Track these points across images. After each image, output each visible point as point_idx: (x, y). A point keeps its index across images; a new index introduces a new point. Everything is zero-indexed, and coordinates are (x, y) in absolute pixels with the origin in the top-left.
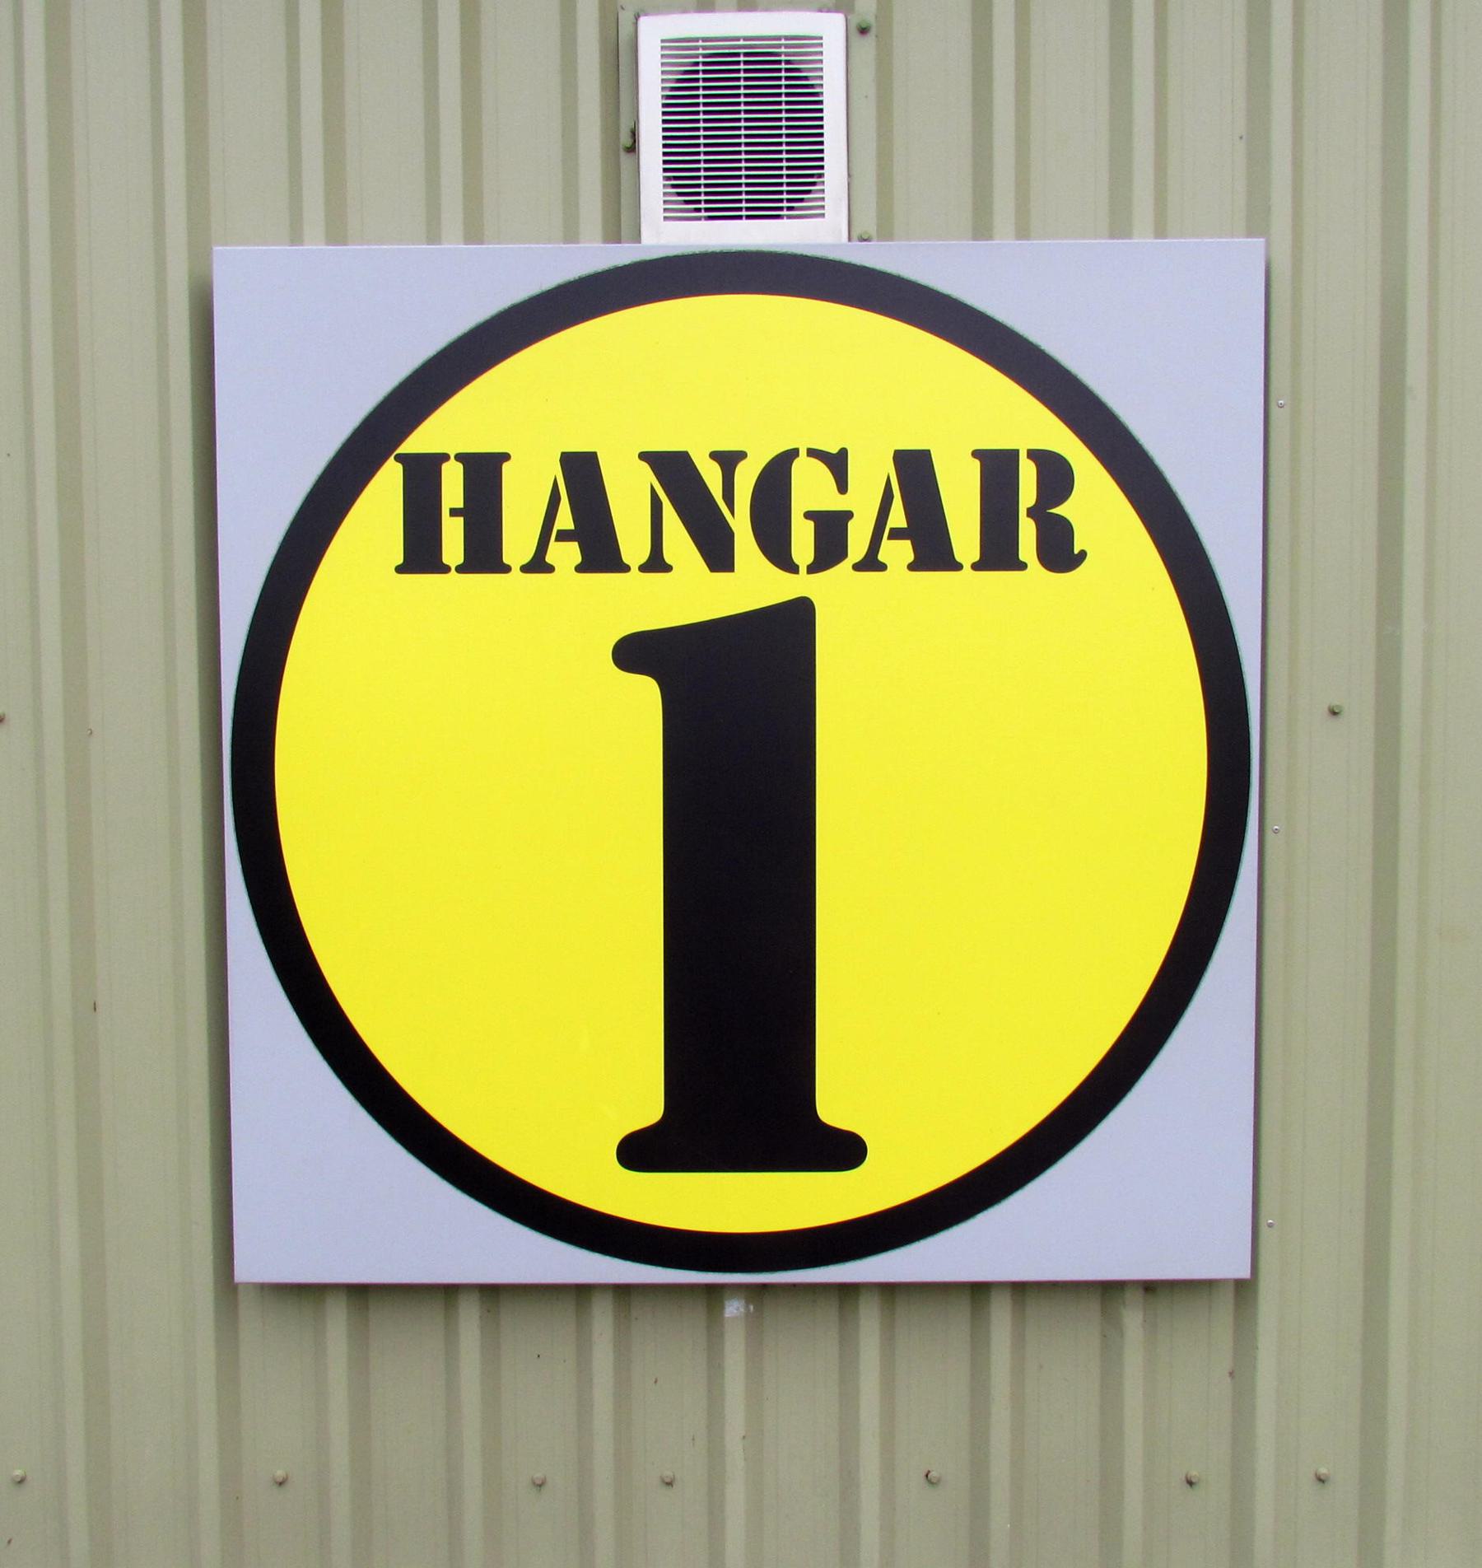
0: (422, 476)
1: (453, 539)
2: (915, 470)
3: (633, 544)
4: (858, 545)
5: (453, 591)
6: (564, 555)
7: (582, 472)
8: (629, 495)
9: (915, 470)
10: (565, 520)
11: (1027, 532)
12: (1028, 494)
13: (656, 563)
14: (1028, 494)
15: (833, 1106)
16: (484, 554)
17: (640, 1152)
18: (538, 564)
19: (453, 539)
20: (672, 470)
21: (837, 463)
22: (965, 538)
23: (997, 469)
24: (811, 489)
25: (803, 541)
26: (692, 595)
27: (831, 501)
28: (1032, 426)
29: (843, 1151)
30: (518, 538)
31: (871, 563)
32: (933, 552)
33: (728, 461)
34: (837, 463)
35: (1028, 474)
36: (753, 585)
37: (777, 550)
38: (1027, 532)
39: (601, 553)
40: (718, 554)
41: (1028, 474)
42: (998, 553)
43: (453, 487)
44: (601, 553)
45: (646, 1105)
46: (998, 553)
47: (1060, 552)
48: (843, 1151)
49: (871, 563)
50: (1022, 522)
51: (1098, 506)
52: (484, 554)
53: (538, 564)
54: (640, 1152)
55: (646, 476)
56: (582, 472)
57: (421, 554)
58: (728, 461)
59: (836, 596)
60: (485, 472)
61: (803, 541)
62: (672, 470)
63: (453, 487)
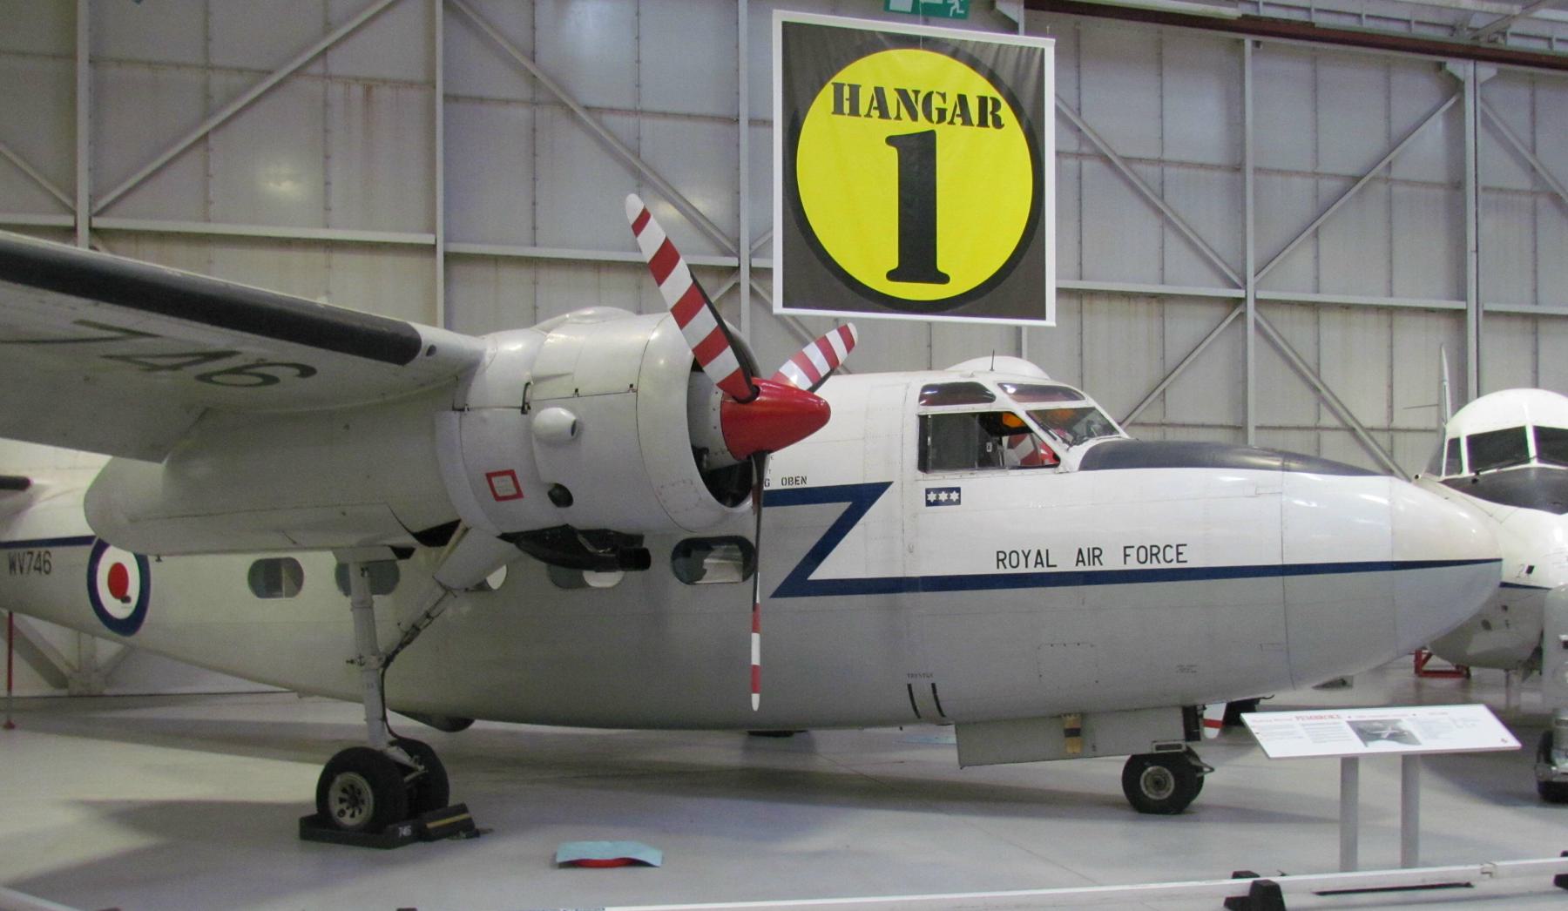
0: (839, 88)
1: (846, 106)
2: (962, 100)
3: (892, 112)
4: (948, 118)
5: (846, 120)
6: (875, 113)
7: (879, 92)
8: (892, 100)
9: (962, 100)
10: (875, 104)
11: (990, 118)
12: (990, 108)
13: (898, 117)
14: (990, 108)
15: (942, 266)
16: (854, 111)
17: (893, 276)
18: (868, 115)
19: (846, 106)
20: (903, 93)
21: (943, 96)
22: (975, 117)
23: (983, 101)
24: (936, 102)
25: (935, 116)
26: (907, 127)
27: (942, 106)
28: (991, 92)
29: (943, 279)
30: (863, 109)
31: (951, 122)
32: (967, 121)
33: (917, 92)
34: (943, 96)
35: (990, 103)
36: (922, 125)
37: (928, 116)
38: (990, 118)
39: (884, 114)
40: (914, 117)
41: (990, 103)
42: (983, 123)
43: (846, 93)
44: (884, 114)
45: (894, 263)
46: (983, 123)
47: (998, 124)
48: (943, 279)
49: (951, 122)
50: (987, 116)
51: (1006, 112)
52: (854, 111)
53: (868, 115)
54: (893, 276)
55: (896, 95)
56: (879, 92)
57: (838, 110)
58: (917, 92)
59: (941, 130)
60: (855, 90)
61: (935, 116)
62: (903, 93)
63: (846, 93)
